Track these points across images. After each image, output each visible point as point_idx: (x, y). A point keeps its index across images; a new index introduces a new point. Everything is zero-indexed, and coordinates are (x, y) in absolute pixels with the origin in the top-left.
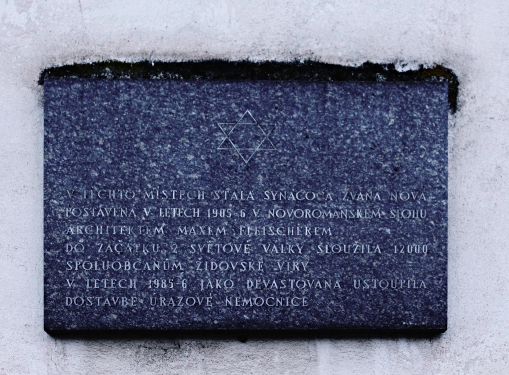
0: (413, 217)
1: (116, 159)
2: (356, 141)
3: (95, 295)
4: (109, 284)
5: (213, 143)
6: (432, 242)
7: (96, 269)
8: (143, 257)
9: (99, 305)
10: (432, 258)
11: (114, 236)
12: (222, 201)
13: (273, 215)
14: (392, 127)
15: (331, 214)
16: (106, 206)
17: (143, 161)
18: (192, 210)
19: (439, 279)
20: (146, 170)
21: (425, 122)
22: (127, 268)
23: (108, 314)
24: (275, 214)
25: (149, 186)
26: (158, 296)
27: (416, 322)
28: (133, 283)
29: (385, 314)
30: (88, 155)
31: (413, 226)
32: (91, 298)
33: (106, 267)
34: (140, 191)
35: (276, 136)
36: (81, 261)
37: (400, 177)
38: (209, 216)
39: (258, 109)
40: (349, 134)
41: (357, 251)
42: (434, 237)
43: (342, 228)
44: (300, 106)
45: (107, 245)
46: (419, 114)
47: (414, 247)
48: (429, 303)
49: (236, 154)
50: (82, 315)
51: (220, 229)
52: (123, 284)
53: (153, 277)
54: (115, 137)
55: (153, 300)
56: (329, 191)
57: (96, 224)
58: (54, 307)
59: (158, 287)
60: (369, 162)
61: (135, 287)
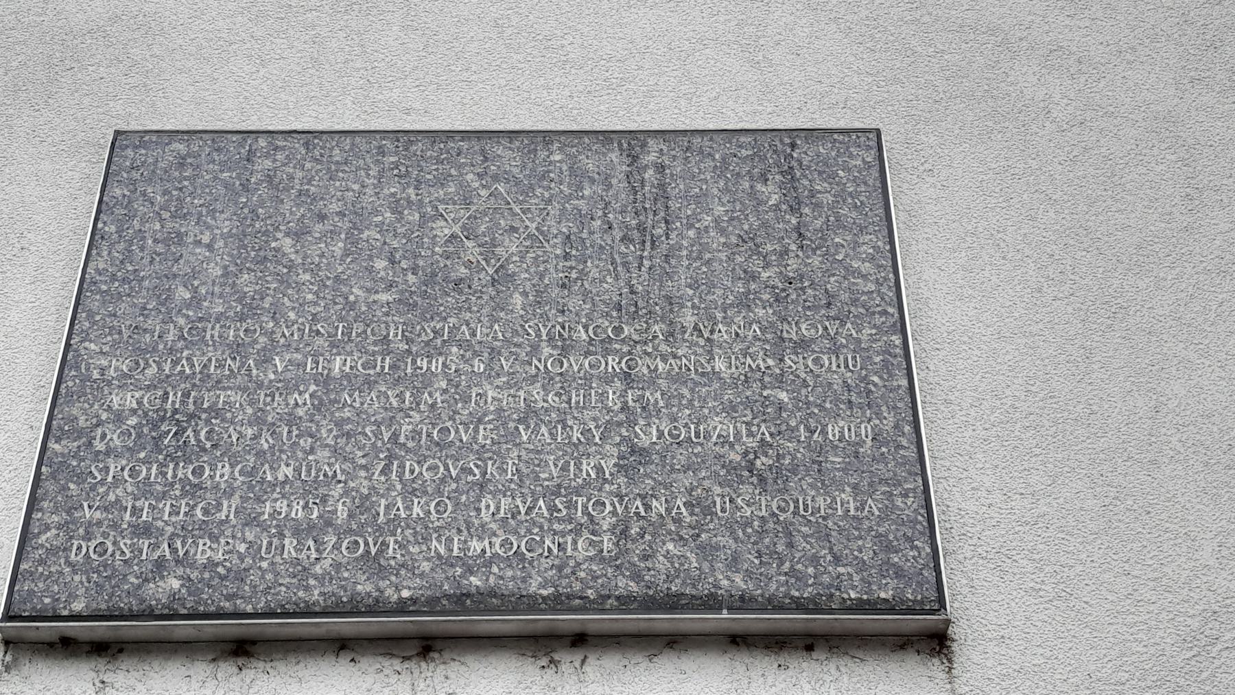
0: (834, 368)
1: (232, 268)
2: (707, 232)
3: (139, 536)
4: (175, 512)
5: (426, 240)
6: (879, 415)
7: (152, 479)
8: (260, 454)
9: (144, 557)
10: (884, 449)
11: (205, 411)
12: (439, 341)
13: (542, 368)
14: (777, 207)
15: (661, 366)
16: (198, 353)
17: (285, 270)
18: (375, 360)
19: (906, 496)
20: (289, 286)
21: (841, 197)
22: (222, 476)
23: (162, 578)
24: (546, 366)
25: (292, 315)
26: (281, 535)
27: (866, 593)
28: (228, 509)
29: (792, 572)
30: (177, 261)
31: (835, 387)
32: (129, 542)
33: (175, 476)
34: (271, 324)
35: (549, 227)
36: (124, 462)
37: (799, 295)
38: (409, 371)
39: (518, 183)
40: (691, 221)
41: (719, 436)
42: (884, 408)
43: (685, 392)
44: (597, 176)
45: (185, 430)
46: (826, 185)
47: (843, 428)
48: (889, 548)
49: (471, 258)
50: (101, 580)
51: (430, 395)
52: (206, 512)
53: (275, 495)
54: (234, 231)
55: (270, 544)
56: (656, 322)
57: (169, 389)
58: (42, 562)
59: (283, 515)
60: (734, 269)
61: (232, 516)
